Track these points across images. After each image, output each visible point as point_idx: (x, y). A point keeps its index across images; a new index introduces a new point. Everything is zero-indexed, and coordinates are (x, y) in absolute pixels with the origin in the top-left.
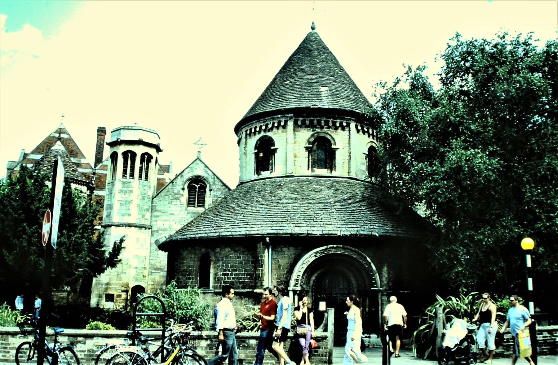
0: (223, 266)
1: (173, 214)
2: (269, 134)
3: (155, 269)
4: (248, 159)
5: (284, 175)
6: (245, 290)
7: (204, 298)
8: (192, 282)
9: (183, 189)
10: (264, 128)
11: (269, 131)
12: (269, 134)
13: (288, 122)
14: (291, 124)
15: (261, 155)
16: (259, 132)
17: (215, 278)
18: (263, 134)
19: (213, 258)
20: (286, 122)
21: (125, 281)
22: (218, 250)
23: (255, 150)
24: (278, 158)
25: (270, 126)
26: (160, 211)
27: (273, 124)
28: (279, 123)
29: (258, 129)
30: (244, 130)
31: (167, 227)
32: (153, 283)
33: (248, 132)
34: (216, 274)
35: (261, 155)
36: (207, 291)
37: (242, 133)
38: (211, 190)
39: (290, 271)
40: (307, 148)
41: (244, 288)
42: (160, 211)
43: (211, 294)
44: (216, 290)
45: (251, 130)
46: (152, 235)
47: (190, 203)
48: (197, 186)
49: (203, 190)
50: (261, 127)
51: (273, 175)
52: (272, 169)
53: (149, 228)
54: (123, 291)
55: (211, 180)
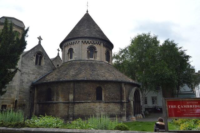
0: (108, 92)
1: (30, 66)
2: (94, 45)
3: (21, 92)
4: (83, 52)
5: (100, 60)
6: (117, 101)
7: (100, 104)
8: (91, 98)
9: (34, 56)
10: (92, 42)
11: (94, 44)
12: (94, 45)
13: (102, 44)
14: (102, 44)
15: (89, 52)
16: (89, 43)
17: (105, 96)
18: (91, 44)
19: (103, 89)
20: (101, 43)
21: (13, 97)
22: (106, 86)
23: (87, 49)
24: (98, 54)
25: (95, 43)
26: (24, 64)
27: (96, 42)
28: (99, 42)
29: (89, 42)
30: (81, 41)
31: (27, 72)
32: (20, 99)
33: (84, 42)
34: (105, 95)
35: (89, 52)
36: (101, 101)
37: (79, 42)
38: (45, 59)
39: (129, 94)
40: (105, 54)
41: (116, 100)
42: (24, 64)
43: (103, 103)
44: (106, 101)
45: (85, 42)
46: (21, 75)
47: (36, 63)
48: (39, 56)
49: (41, 58)
50: (91, 42)
51: (96, 60)
52: (95, 58)
53: (21, 71)
54: (11, 103)
55: (45, 55)
